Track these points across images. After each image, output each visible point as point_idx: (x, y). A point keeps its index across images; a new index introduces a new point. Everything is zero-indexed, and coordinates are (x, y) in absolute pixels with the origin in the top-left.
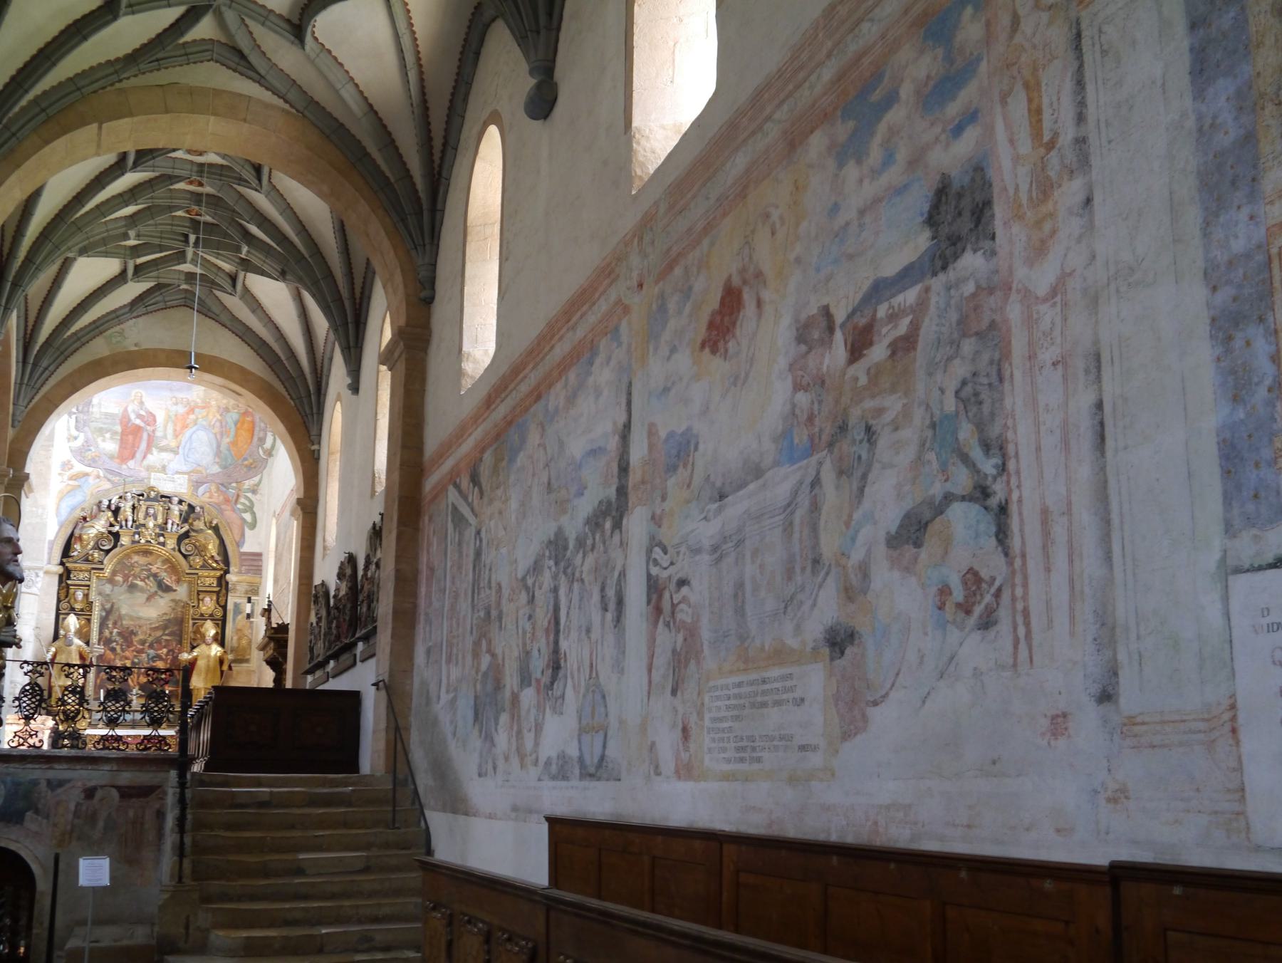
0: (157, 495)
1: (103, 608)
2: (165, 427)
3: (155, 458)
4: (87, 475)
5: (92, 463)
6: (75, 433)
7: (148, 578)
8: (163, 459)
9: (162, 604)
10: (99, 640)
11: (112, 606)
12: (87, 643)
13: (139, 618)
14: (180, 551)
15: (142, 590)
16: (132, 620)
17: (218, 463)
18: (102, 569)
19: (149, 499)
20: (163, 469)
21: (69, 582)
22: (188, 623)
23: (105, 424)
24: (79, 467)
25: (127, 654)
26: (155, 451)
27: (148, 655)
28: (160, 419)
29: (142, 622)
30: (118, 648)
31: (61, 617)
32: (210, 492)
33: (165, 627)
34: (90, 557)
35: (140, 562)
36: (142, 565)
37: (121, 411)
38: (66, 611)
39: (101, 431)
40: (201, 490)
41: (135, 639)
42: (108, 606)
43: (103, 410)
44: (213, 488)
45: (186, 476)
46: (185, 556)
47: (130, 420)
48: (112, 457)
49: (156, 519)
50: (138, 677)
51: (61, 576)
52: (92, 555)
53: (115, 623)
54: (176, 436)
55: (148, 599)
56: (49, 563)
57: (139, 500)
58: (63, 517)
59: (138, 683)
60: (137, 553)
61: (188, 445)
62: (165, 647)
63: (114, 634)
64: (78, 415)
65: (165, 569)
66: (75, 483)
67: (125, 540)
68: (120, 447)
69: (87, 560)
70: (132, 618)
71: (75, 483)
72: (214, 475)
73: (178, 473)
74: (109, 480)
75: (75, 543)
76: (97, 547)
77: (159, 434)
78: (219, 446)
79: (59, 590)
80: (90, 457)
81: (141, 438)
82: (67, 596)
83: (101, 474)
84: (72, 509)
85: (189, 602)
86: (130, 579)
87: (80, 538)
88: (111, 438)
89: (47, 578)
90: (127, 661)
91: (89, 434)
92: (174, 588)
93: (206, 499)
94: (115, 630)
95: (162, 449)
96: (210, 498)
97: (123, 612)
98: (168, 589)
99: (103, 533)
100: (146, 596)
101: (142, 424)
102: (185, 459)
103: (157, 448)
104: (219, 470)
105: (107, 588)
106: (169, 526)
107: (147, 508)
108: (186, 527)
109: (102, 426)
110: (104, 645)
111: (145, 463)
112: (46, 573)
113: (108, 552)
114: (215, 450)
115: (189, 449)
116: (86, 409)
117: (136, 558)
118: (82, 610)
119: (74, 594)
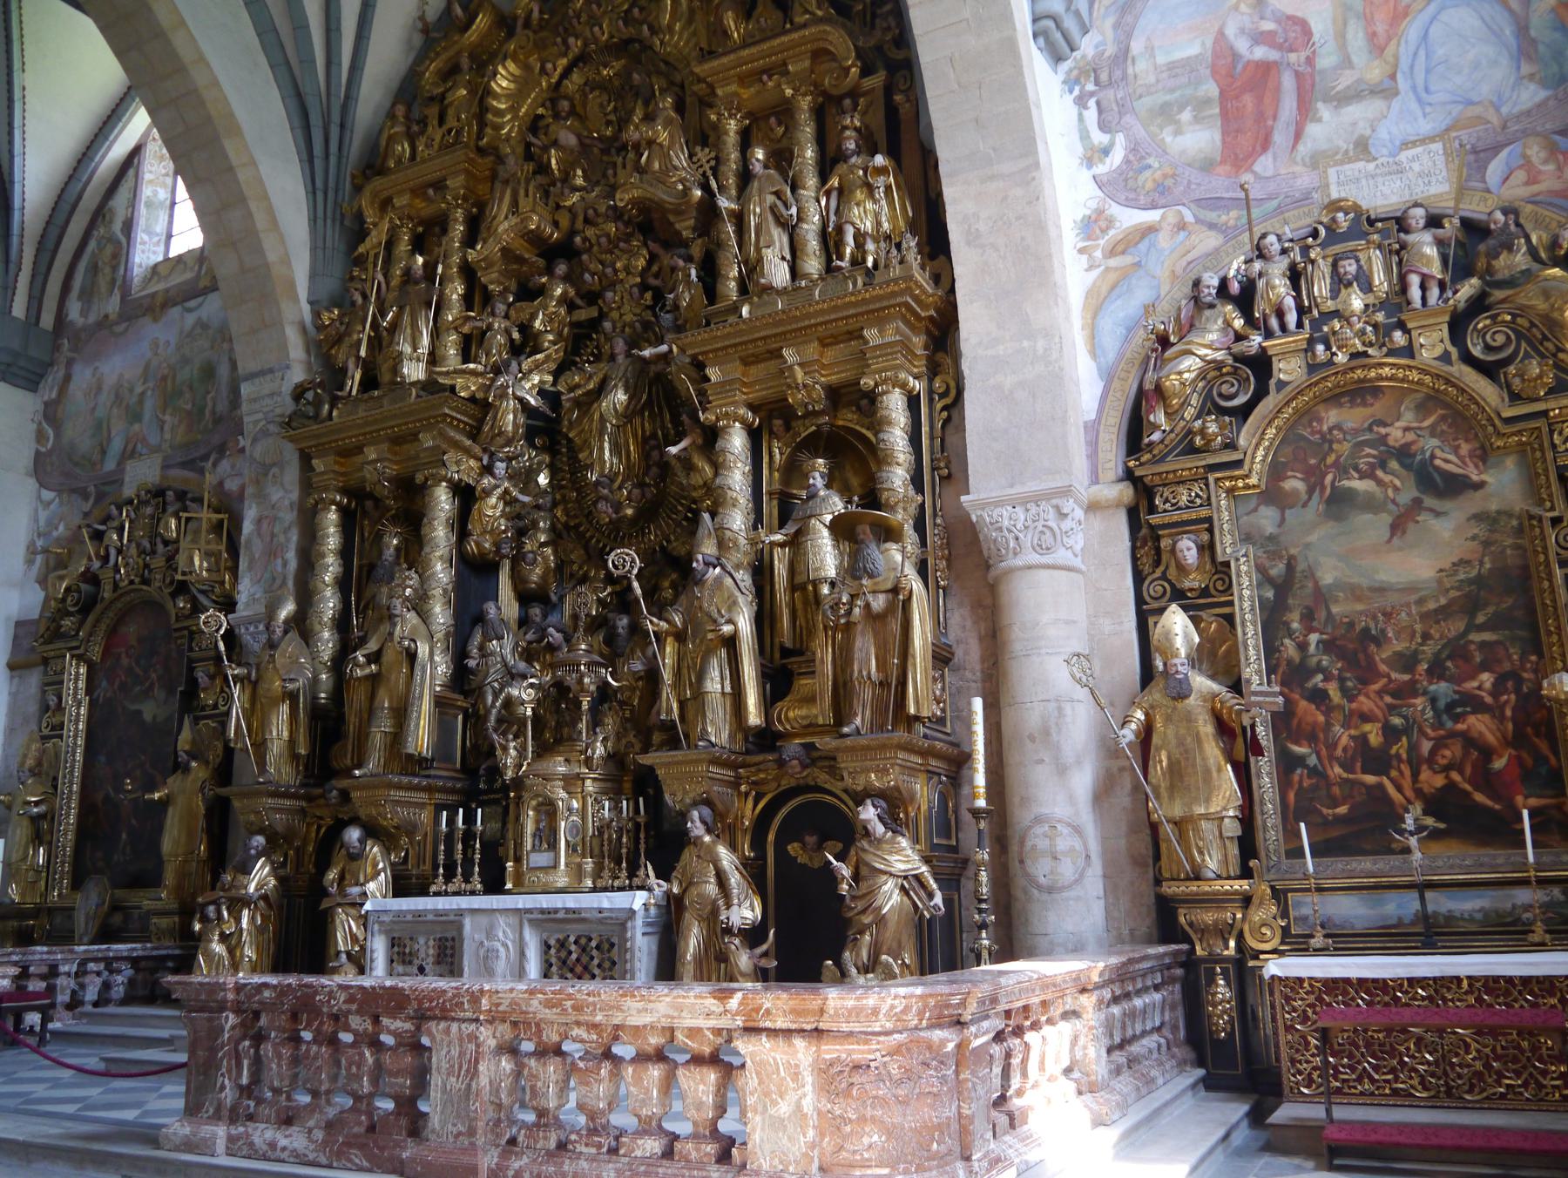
0: (1356, 220)
1: (1265, 578)
2: (1341, 37)
3: (1327, 127)
4: (1149, 230)
5: (1159, 196)
6: (1099, 138)
7: (1383, 465)
8: (1354, 124)
9: (1446, 535)
10: (1271, 670)
11: (1290, 567)
12: (1237, 687)
13: (1381, 590)
14: (1468, 359)
15: (1371, 505)
16: (1359, 599)
17: (1531, 77)
18: (1238, 464)
19: (1334, 236)
20: (1362, 148)
21: (1155, 519)
22: (1550, 576)
23: (1172, 90)
24: (1130, 218)
25: (1365, 703)
26: (1324, 111)
27: (1433, 701)
28: (1320, 26)
29: (1393, 599)
30: (1333, 690)
31: (1151, 621)
32: (1527, 164)
33: (1469, 602)
34: (1198, 441)
35: (1349, 425)
36: (1356, 432)
37: (1209, 43)
38: (1162, 603)
39: (1166, 113)
40: (1495, 169)
41: (1381, 656)
42: (1278, 570)
43: (1161, 59)
44: (1536, 152)
45: (1437, 147)
46: (1488, 370)
47: (1235, 56)
48: (1207, 166)
49: (1367, 287)
50: (1415, 775)
51: (1133, 514)
52: (1202, 432)
53: (1308, 617)
54: (1377, 47)
55: (1397, 527)
56: (1095, 480)
57: (1305, 250)
58: (1111, 356)
59: (1419, 793)
60: (1333, 398)
61: (1422, 53)
62: (1484, 667)
63: (1312, 648)
64: (1101, 95)
65: (1433, 428)
66: (1127, 260)
67: (1288, 370)
68: (1225, 133)
69: (1192, 450)
70: (1355, 593)
71: (1127, 260)
72: (1528, 113)
73: (1406, 145)
74: (1212, 226)
75: (1151, 410)
76: (1212, 406)
77: (1326, 61)
78: (1522, 29)
79: (1134, 549)
80: (1149, 185)
81: (1278, 89)
82: (1157, 563)
83: (1189, 217)
84: (1129, 330)
85: (1536, 511)
86: (1329, 478)
87: (1159, 390)
88: (1197, 120)
89: (1097, 522)
90: (1367, 727)
91: (1140, 132)
92: (1475, 478)
93: (1516, 191)
94: (1314, 638)
95: (1343, 99)
96: (1531, 181)
97: (1327, 578)
98: (1454, 486)
99: (1219, 365)
100: (1386, 519)
101: (1273, 55)
102: (1419, 100)
103: (1326, 100)
104: (1543, 94)
105: (1267, 519)
106: (1415, 293)
107: (1335, 265)
108: (1468, 289)
109: (1168, 98)
110: (1283, 684)
111: (1304, 148)
112: (1092, 507)
113: (1244, 412)
114: (1512, 41)
115: (1428, 71)
116: (1118, 73)
117: (1332, 416)
118: (1205, 592)
119: (1173, 551)
